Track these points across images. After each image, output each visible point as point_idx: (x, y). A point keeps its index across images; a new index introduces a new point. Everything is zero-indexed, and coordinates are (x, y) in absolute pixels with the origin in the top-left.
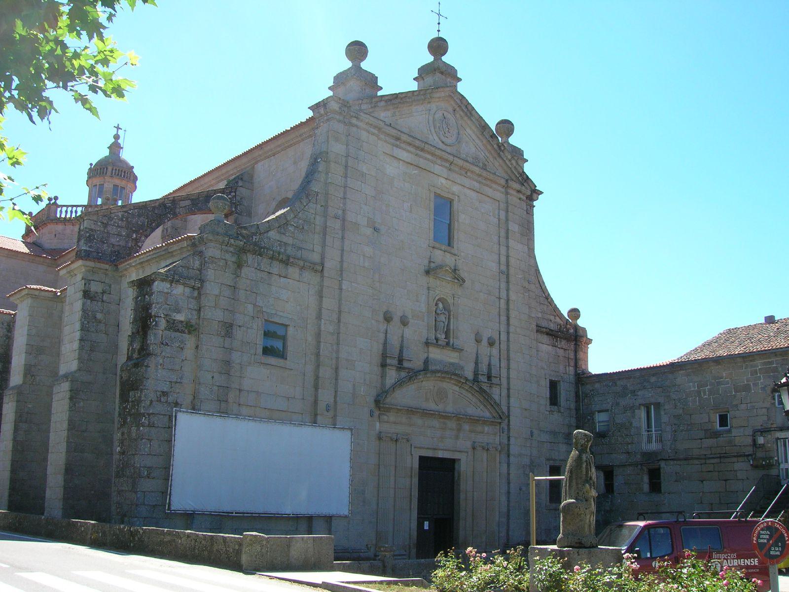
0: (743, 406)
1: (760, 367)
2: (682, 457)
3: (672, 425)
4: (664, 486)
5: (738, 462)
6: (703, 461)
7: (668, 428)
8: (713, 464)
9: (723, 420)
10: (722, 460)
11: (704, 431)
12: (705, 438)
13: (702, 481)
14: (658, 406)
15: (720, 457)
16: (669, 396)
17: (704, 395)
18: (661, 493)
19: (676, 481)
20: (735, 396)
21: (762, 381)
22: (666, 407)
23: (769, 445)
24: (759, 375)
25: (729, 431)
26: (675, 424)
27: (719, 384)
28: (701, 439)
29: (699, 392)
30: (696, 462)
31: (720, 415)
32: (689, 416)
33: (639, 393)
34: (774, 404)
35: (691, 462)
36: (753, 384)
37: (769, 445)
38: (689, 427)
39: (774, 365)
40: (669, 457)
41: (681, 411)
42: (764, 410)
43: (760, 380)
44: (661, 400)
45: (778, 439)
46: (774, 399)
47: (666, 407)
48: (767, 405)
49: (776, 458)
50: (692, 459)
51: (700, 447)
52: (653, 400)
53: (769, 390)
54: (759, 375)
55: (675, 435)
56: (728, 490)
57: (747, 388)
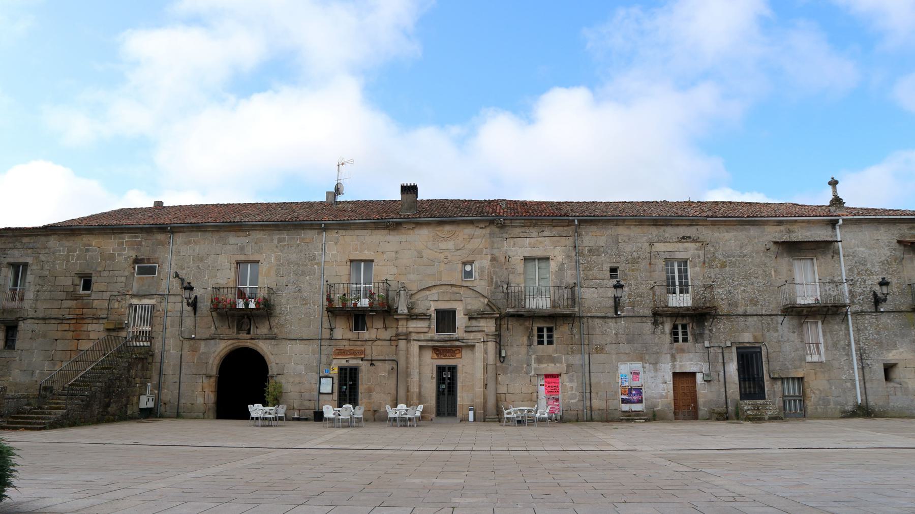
0: (106, 274)
1: (127, 240)
2: (40, 316)
3: (36, 285)
4: (18, 344)
5: (92, 323)
6: (60, 321)
7: (33, 288)
8: (69, 324)
9: (87, 285)
10: (78, 321)
11: (65, 293)
12: (66, 300)
13: (56, 340)
14: (26, 265)
15: (76, 319)
16: (39, 257)
17: (72, 260)
18: (14, 349)
19: (31, 339)
20: (100, 263)
21: (126, 252)
22: (34, 267)
23: (123, 310)
24: (124, 246)
25: (89, 295)
26: (39, 285)
27: (87, 250)
28: (62, 300)
29: (68, 256)
30: (53, 321)
31: (84, 280)
32: (54, 278)
33: (9, 252)
34: (134, 273)
35: (47, 322)
36: (118, 254)
37: (123, 310)
38: (52, 289)
39: (140, 239)
40: (28, 315)
41: (48, 273)
42: (123, 279)
43: (125, 251)
44: (29, 260)
45: (131, 305)
46: (134, 269)
47: (34, 267)
48: (126, 273)
49: (126, 322)
50: (50, 318)
51: (59, 307)
52: (21, 260)
53: (131, 261)
54: (124, 246)
55: (37, 295)
56: (79, 349)
57: (112, 257)
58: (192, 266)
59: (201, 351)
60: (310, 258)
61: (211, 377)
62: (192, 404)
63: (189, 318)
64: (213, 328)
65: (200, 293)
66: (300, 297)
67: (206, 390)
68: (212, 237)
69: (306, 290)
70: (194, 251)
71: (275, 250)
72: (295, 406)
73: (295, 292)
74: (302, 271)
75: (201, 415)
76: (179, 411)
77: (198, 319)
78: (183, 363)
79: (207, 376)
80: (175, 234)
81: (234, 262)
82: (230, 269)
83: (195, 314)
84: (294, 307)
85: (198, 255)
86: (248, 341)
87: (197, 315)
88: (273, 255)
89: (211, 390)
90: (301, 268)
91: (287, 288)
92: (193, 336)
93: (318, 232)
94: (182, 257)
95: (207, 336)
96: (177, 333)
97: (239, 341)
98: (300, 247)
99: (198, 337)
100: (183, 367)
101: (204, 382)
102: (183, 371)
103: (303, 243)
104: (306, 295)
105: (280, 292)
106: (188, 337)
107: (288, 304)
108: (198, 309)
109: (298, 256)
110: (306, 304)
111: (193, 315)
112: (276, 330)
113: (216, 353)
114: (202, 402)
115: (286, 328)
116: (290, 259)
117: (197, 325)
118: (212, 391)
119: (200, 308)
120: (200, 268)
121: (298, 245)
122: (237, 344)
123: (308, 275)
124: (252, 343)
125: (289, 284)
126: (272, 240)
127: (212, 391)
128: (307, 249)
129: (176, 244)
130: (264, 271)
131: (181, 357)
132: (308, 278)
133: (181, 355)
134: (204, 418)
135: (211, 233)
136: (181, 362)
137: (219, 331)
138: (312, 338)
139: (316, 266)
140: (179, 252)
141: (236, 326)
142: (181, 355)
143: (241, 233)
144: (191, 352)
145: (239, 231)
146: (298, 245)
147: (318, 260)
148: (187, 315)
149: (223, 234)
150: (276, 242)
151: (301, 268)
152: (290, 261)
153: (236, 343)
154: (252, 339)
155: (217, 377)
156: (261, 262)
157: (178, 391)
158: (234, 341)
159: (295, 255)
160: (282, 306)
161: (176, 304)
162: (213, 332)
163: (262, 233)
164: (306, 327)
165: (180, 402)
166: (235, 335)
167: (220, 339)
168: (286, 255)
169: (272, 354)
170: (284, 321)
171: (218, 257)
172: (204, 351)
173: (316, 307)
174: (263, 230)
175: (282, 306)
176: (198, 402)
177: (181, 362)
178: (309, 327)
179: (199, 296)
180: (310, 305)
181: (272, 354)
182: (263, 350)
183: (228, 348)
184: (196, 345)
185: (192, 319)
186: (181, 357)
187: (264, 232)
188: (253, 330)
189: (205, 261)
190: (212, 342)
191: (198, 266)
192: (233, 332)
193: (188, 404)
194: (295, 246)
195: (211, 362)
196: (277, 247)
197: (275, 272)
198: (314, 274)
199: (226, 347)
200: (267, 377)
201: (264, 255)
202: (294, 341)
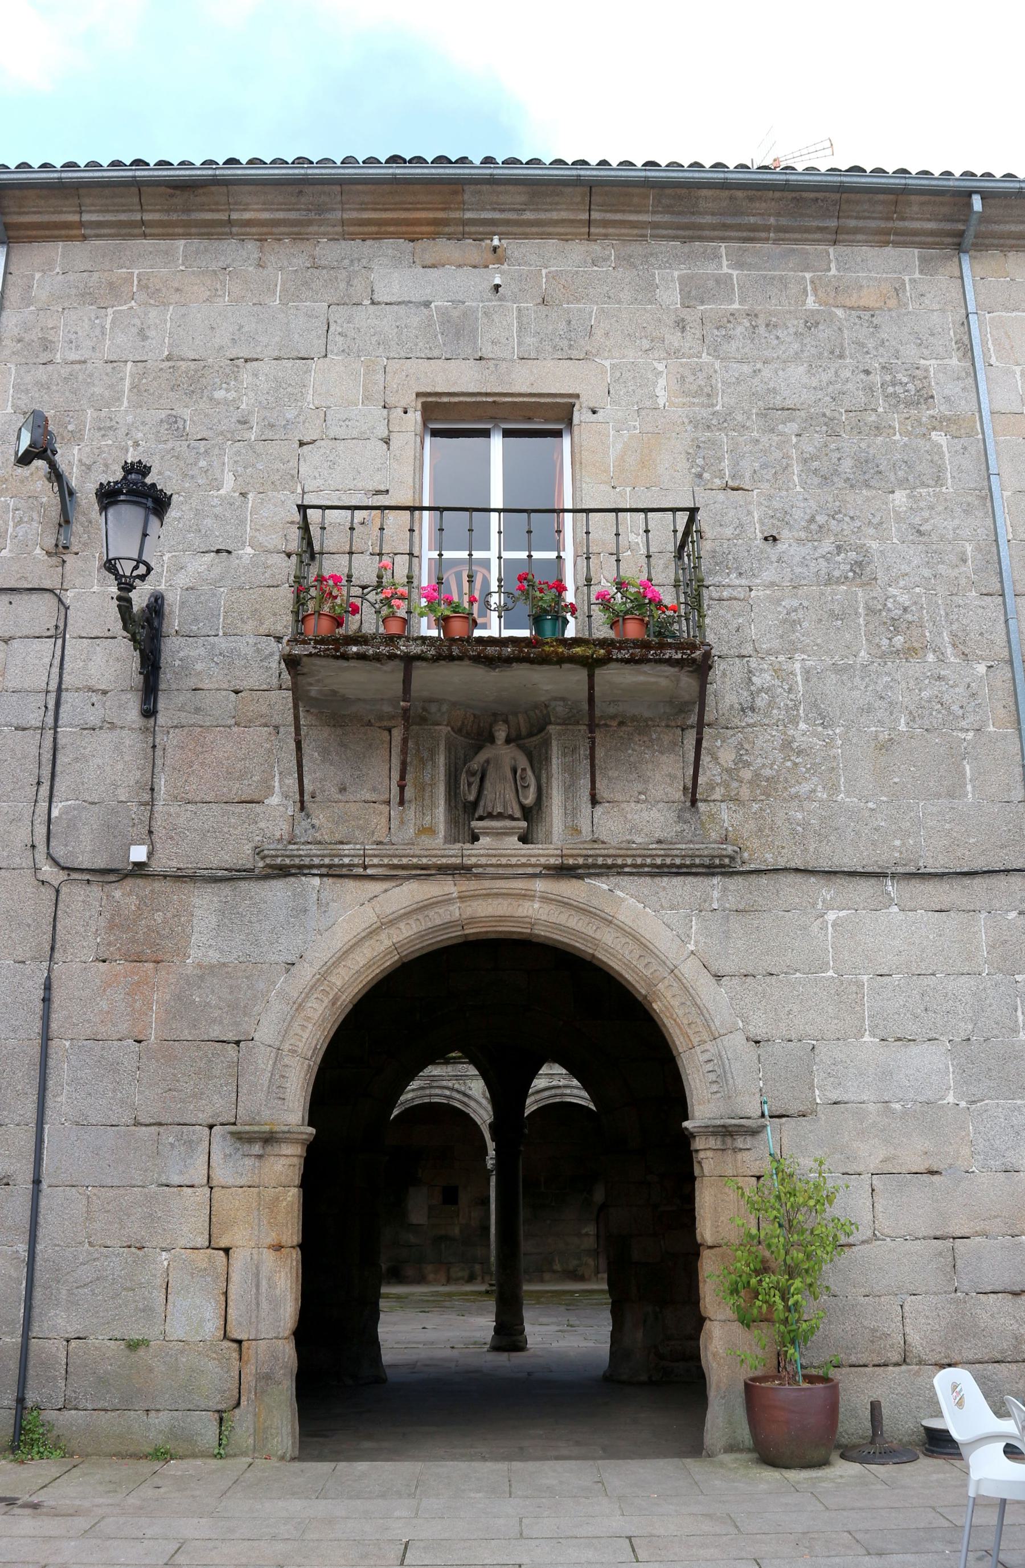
58: (130, 419)
59: (194, 955)
60: (899, 389)
61: (269, 1139)
62: (133, 1346)
63: (106, 737)
64: (275, 800)
65: (182, 580)
66: (870, 611)
67: (237, 1237)
68: (260, 265)
69: (907, 569)
70: (142, 334)
71: (674, 339)
72: (915, 1339)
73: (829, 581)
74: (862, 462)
75: (207, 1430)
76: (32, 1397)
77: (170, 740)
78: (59, 1046)
79: (242, 1138)
80: (18, 249)
81: (409, 399)
82: (387, 441)
83: (149, 712)
84: (838, 670)
85: (168, 359)
86: (540, 886)
87: (161, 719)
88: (660, 367)
89: (272, 1238)
90: (849, 442)
91: (773, 552)
92: (138, 853)
93: (923, 259)
94: (65, 371)
95: (243, 855)
96: (22, 835)
97: (473, 885)
98: (824, 332)
99: (156, 867)
100: (61, 1071)
101: (220, 1175)
102: (59, 1101)
103: (840, 312)
104: (905, 599)
105: (733, 579)
106: (100, 863)
107: (792, 650)
108: (166, 678)
109: (825, 377)
110: (910, 652)
111: (132, 714)
112: (727, 816)
113: (307, 973)
114: (212, 1328)
115: (796, 796)
116: (774, 391)
117: (162, 784)
118: (278, 1247)
119: (186, 669)
120: (182, 435)
121: (811, 323)
122: (455, 912)
123: (903, 483)
124: (565, 904)
125: (785, 534)
126: (651, 287)
127: (278, 1247)
128: (871, 344)
129: (27, 300)
130: (613, 454)
131: (47, 1000)
132: (900, 497)
133: (48, 987)
134: (222, 1450)
135: (251, 246)
136: (46, 1038)
137: (320, 818)
138: (979, 864)
139: (939, 437)
140: (46, 345)
141: (441, 790)
142: (48, 987)
143: (443, 248)
144: (120, 967)
145: (437, 230)
146: (811, 323)
147: (947, 399)
148: (93, 717)
149: (329, 251)
150: (671, 296)
151: (849, 442)
152: (778, 401)
153: (446, 901)
154: (563, 871)
155: (301, 1156)
156: (587, 400)
157: (22, 1248)
158: (448, 887)
159: (798, 372)
160: (753, 663)
161: (15, 644)
162: (280, 829)
163: (578, 251)
164: (938, 795)
165: (35, 1330)
166: (453, 853)
167: (334, 872)
168: (746, 369)
169: (718, 977)
170: (779, 756)
171: (308, 371)
172: (214, 956)
173: (981, 669)
174: (588, 231)
175: (753, 663)
176: (177, 1329)
177: (46, 1038)
178: (954, 792)
179: (173, 600)
180: (941, 660)
181: (718, 977)
182: (645, 947)
183: (386, 941)
184: (159, 917)
185: (131, 741)
186: (47, 1000)
187: (596, 247)
188: (570, 812)
189: (220, 394)
190: (278, 890)
191: (173, 420)
192: (431, 831)
193: (98, 1340)
194: (796, 324)
195: (266, 1032)
196: (681, 325)
197: (683, 464)
198: (939, 481)
199: (372, 933)
200: (685, 1139)
201: (607, 363)
202: (865, 888)
